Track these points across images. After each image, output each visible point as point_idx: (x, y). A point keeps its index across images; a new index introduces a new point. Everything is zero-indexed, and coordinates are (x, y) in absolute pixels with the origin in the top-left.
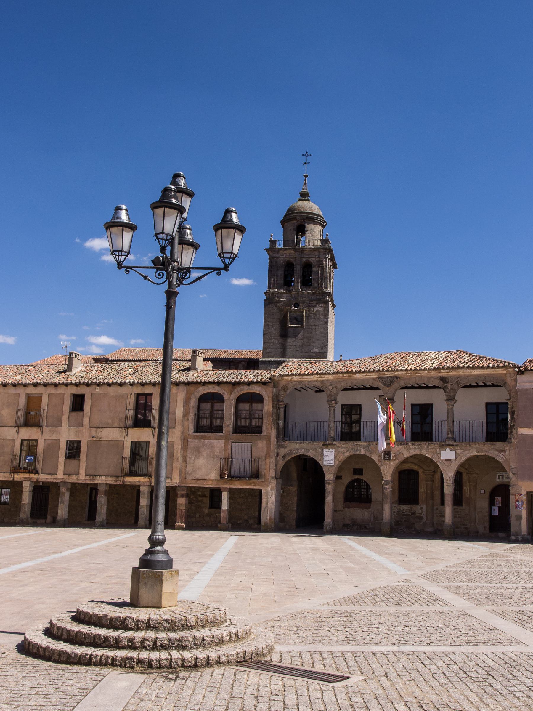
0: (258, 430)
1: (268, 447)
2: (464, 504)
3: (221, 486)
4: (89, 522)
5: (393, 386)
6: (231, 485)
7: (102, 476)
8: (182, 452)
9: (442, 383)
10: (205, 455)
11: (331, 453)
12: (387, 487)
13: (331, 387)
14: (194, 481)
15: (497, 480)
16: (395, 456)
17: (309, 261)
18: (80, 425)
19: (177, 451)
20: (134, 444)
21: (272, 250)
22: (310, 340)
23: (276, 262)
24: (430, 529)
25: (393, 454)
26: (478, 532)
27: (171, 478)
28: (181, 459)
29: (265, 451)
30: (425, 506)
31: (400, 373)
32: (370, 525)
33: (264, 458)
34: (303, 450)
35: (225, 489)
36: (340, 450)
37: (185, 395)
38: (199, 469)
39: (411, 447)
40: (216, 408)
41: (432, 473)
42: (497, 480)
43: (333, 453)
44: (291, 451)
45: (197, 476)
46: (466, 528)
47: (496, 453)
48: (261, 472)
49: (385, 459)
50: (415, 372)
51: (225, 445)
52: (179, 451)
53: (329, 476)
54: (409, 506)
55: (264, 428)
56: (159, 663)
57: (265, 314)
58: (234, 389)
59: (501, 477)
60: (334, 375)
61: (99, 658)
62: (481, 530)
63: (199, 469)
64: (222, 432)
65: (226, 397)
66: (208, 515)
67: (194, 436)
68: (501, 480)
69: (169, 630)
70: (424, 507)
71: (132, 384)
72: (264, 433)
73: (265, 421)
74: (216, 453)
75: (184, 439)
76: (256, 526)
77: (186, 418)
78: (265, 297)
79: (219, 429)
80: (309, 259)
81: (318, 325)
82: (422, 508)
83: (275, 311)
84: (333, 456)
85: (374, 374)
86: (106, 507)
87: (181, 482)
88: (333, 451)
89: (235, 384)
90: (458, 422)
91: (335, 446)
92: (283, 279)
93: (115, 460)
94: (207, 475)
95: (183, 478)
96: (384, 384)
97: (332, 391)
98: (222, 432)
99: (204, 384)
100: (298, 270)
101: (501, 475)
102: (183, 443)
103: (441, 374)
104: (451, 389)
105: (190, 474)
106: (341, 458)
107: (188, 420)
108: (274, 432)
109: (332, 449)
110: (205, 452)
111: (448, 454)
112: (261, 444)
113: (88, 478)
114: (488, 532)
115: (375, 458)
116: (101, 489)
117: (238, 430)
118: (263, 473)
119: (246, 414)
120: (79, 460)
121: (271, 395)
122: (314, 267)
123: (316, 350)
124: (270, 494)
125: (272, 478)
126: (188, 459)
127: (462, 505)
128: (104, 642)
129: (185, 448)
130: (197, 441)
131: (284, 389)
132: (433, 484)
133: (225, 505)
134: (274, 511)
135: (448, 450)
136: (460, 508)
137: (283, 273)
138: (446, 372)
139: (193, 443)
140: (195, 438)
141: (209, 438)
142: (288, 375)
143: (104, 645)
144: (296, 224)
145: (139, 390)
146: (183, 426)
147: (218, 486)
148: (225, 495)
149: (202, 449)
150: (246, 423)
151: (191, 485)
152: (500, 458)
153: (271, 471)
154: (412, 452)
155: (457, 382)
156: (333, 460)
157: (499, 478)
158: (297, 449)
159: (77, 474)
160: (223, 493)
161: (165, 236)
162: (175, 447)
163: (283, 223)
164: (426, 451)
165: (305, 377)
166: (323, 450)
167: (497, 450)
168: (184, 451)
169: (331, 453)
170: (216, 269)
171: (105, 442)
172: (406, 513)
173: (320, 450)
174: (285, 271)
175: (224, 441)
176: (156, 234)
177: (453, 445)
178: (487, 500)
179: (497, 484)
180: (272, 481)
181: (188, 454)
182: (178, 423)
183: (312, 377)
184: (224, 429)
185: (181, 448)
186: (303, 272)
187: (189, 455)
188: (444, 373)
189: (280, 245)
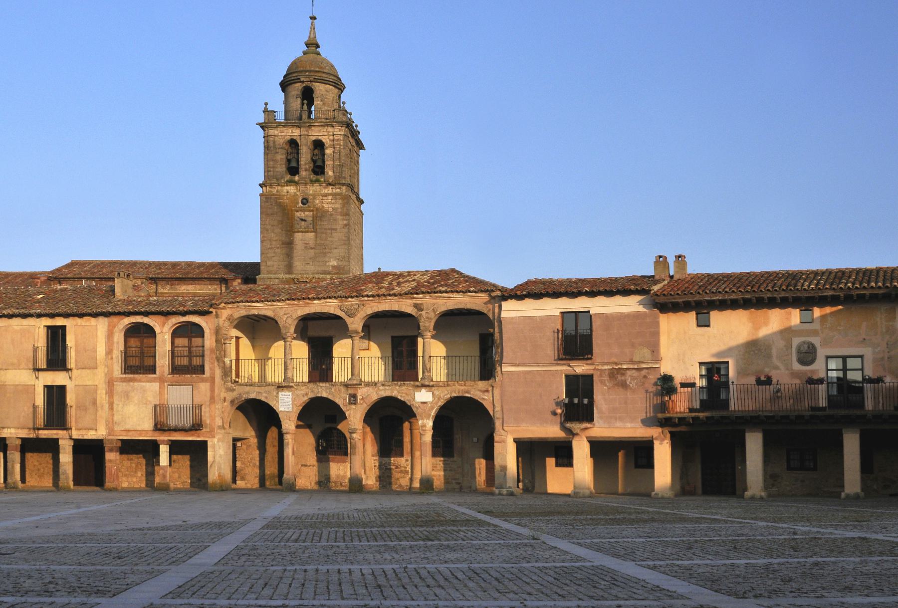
1: (212, 390)
7: (10, 428)
8: (107, 398)
10: (136, 402)
14: (124, 433)
16: (363, 399)
19: (101, 397)
20: (49, 389)
23: (274, 142)
25: (359, 397)
27: (96, 430)
28: (106, 406)
29: (208, 394)
33: (208, 403)
34: (255, 393)
38: (129, 417)
43: (291, 397)
44: (240, 394)
45: (128, 427)
47: (478, 393)
48: (205, 420)
49: (350, 403)
51: (160, 388)
52: (104, 396)
55: (207, 368)
57: (261, 213)
63: (129, 417)
64: (155, 373)
67: (122, 378)
73: (207, 359)
74: (149, 399)
75: (109, 382)
79: (152, 369)
80: (320, 138)
81: (335, 229)
83: (275, 210)
84: (290, 400)
87: (109, 434)
88: (290, 394)
90: (435, 358)
91: (293, 389)
92: (284, 166)
93: (26, 409)
94: (139, 425)
95: (111, 431)
97: (287, 321)
98: (155, 373)
102: (109, 387)
103: (415, 301)
104: (427, 318)
105: (119, 424)
108: (218, 373)
109: (289, 391)
110: (136, 397)
112: (204, 387)
115: (339, 401)
117: (176, 369)
118: (208, 422)
122: (327, 148)
126: (115, 406)
129: (110, 392)
130: (124, 384)
135: (423, 390)
137: (284, 157)
139: (119, 387)
140: (123, 380)
141: (140, 381)
146: (106, 366)
149: (132, 394)
150: (184, 361)
153: (217, 419)
156: (291, 406)
158: (248, 393)
162: (99, 392)
164: (399, 392)
166: (278, 393)
167: (481, 391)
168: (109, 397)
171: (12, 387)
173: (275, 394)
175: (158, 383)
177: (428, 386)
180: (218, 431)
182: (101, 362)
184: (157, 369)
185: (106, 393)
187: (116, 402)
189: (280, 117)
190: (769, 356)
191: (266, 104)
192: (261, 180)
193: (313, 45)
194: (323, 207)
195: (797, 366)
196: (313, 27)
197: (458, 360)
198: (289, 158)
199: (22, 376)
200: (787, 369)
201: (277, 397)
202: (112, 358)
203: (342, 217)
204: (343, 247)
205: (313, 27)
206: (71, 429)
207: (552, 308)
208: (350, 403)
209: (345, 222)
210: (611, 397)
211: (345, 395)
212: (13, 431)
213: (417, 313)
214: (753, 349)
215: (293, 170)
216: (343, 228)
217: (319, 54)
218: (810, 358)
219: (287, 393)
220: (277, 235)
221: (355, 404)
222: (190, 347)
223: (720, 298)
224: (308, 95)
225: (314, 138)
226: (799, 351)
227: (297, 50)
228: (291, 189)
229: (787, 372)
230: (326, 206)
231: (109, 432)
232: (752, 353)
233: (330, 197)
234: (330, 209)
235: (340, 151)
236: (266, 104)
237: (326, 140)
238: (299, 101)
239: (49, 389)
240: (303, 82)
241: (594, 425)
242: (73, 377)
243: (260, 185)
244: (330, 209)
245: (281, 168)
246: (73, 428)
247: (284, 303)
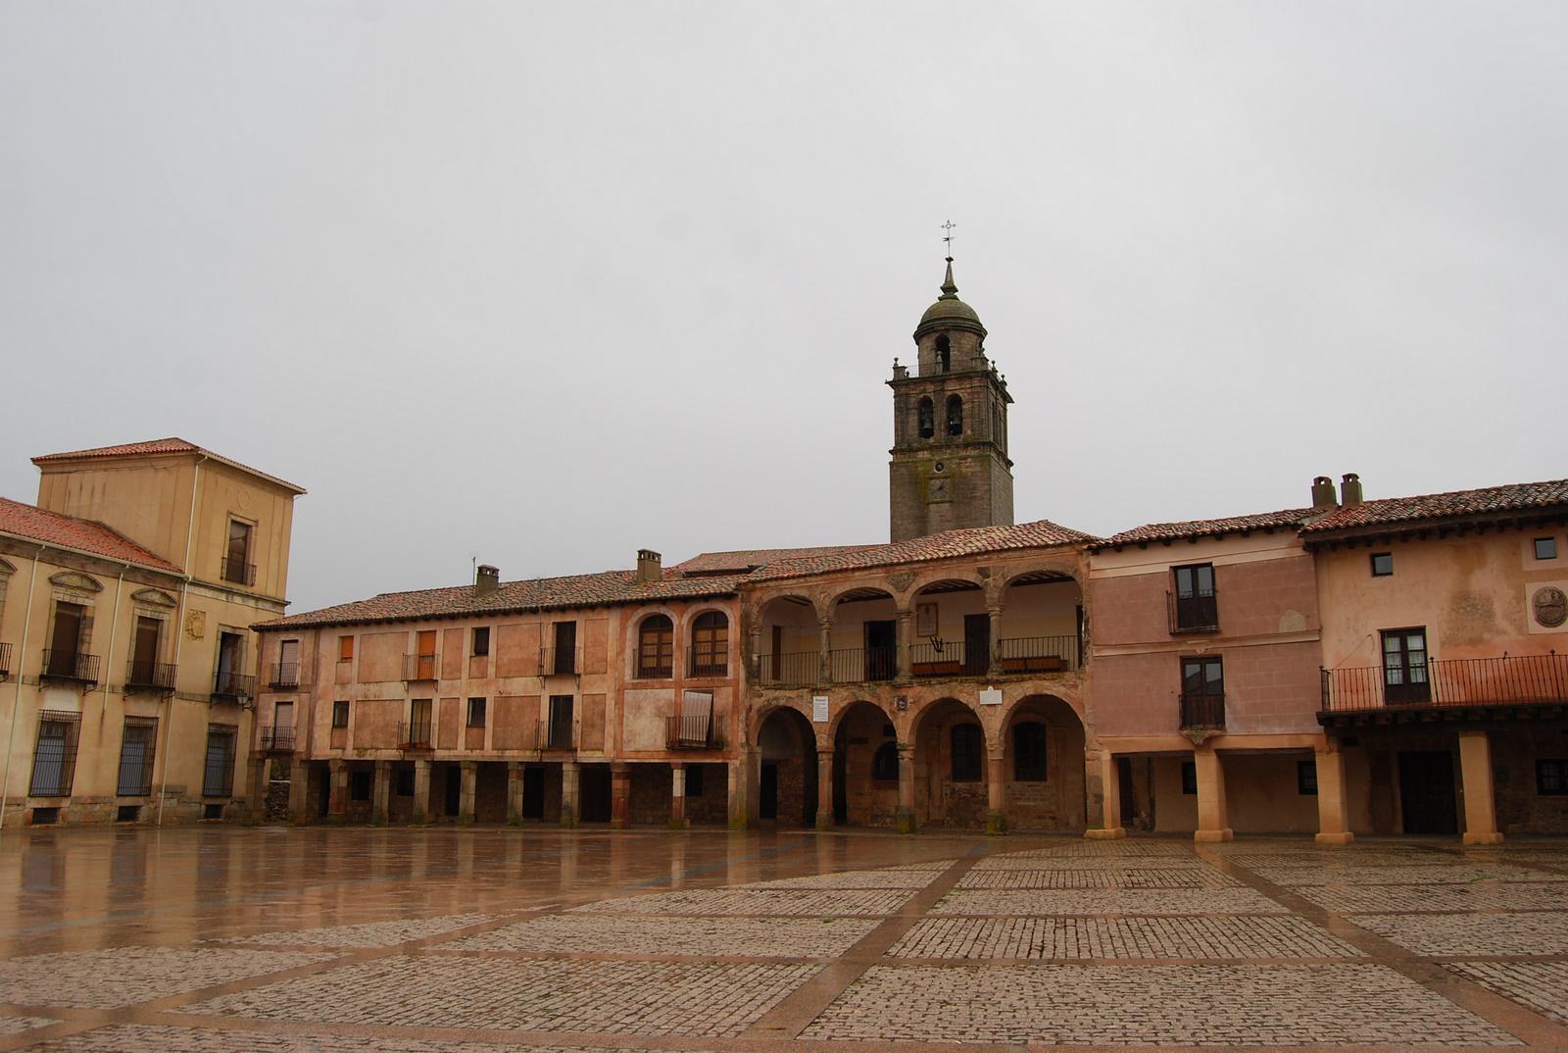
3: (671, 761)
6: (685, 758)
10: (648, 714)
13: (822, 596)
16: (914, 702)
17: (957, 395)
18: (483, 675)
20: (554, 699)
21: (900, 382)
25: (910, 700)
27: (603, 751)
33: (730, 713)
35: (677, 766)
43: (827, 702)
49: (900, 710)
53: (823, 741)
54: (968, 784)
60: (824, 577)
64: (671, 677)
67: (633, 684)
72: (730, 676)
77: (621, 657)
78: (891, 458)
80: (957, 392)
84: (827, 706)
85: (880, 570)
89: (685, 600)
90: (1006, 642)
92: (916, 428)
96: (896, 587)
98: (671, 677)
107: (624, 660)
108: (742, 674)
111: (990, 696)
113: (495, 753)
118: (730, 739)
119: (707, 648)
120: (484, 727)
121: (738, 615)
125: (742, 746)
127: (1045, 780)
129: (620, 703)
134: (745, 798)
135: (990, 688)
136: (1043, 783)
140: (635, 687)
142: (760, 581)
145: (559, 618)
147: (666, 761)
151: (629, 761)
153: (740, 734)
158: (776, 699)
159: (482, 748)
160: (675, 771)
163: (918, 337)
172: (963, 796)
190: (1489, 614)
191: (896, 360)
193: (949, 289)
194: (961, 471)
195: (1536, 628)
196: (949, 267)
197: (1046, 644)
199: (522, 685)
200: (1521, 634)
201: (812, 703)
205: (949, 267)
206: (576, 750)
207: (1159, 563)
210: (1249, 688)
212: (516, 751)
214: (1463, 604)
215: (927, 433)
217: (956, 298)
218: (1558, 615)
219: (823, 698)
223: (1404, 529)
224: (943, 346)
225: (949, 393)
226: (1538, 606)
227: (933, 296)
229: (1521, 637)
230: (964, 470)
232: (1461, 611)
234: (969, 474)
236: (896, 360)
239: (554, 699)
241: (1225, 731)
242: (581, 684)
243: (890, 452)
244: (969, 474)
246: (579, 749)
247: (820, 578)
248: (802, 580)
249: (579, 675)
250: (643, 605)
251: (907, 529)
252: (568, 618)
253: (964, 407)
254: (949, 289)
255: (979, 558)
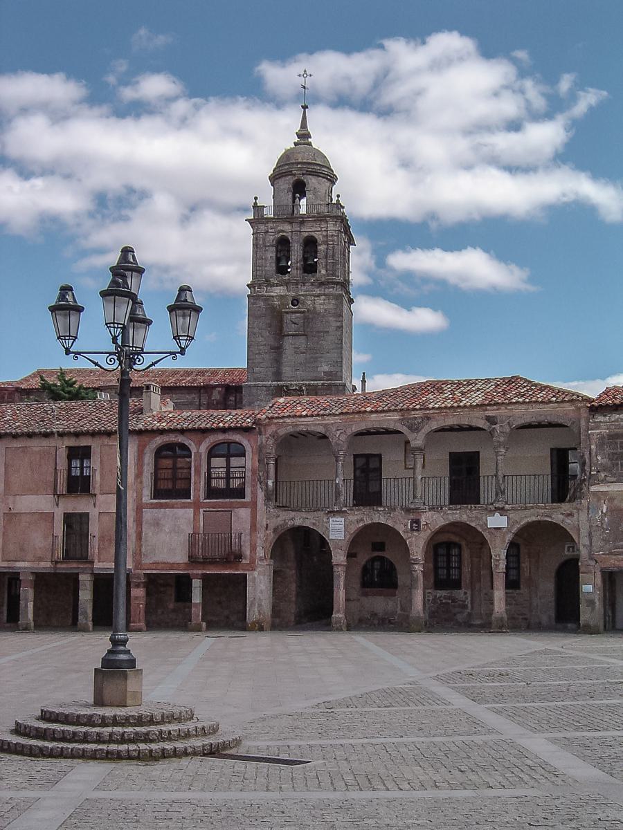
0: (240, 493)
2: (522, 586)
3: (190, 572)
4: (8, 625)
5: (423, 431)
9: (488, 424)
11: (341, 523)
12: (416, 567)
15: (566, 553)
17: (313, 237)
22: (317, 353)
24: (478, 622)
25: (423, 523)
26: (540, 623)
30: (470, 590)
31: (432, 411)
32: (396, 618)
35: (196, 576)
36: (351, 518)
37: (136, 448)
39: (449, 512)
40: (179, 465)
41: (480, 546)
42: (566, 553)
46: (526, 619)
49: (412, 530)
50: (452, 411)
51: (195, 514)
53: (339, 557)
54: (449, 591)
55: (248, 491)
56: (129, 754)
58: (205, 438)
59: (571, 548)
60: (342, 417)
61: (70, 750)
62: (545, 619)
64: (190, 498)
65: (193, 449)
66: (174, 611)
67: (152, 504)
68: (571, 553)
69: (135, 726)
70: (469, 592)
71: (61, 435)
72: (248, 499)
75: (137, 509)
76: (240, 624)
80: (313, 234)
81: (328, 332)
82: (465, 593)
84: (343, 526)
85: (395, 413)
86: (32, 603)
89: (205, 432)
92: (274, 265)
95: (138, 565)
96: (410, 428)
98: (190, 498)
99: (162, 432)
100: (297, 251)
101: (571, 547)
103: (487, 413)
106: (353, 528)
108: (261, 495)
111: (497, 521)
114: (554, 623)
115: (401, 529)
116: (26, 578)
117: (212, 493)
119: (221, 472)
122: (320, 245)
123: (326, 368)
124: (257, 580)
127: (519, 588)
128: (73, 737)
131: (274, 437)
132: (480, 561)
133: (197, 598)
137: (274, 255)
138: (494, 410)
142: (278, 418)
143: (73, 740)
144: (291, 182)
145: (72, 442)
148: (197, 584)
152: (568, 524)
154: (452, 518)
155: (508, 422)
157: (568, 550)
161: (116, 325)
165: (303, 419)
166: (328, 518)
168: (137, 525)
169: (341, 523)
170: (171, 353)
172: (444, 601)
174: (277, 251)
176: (106, 324)
178: (553, 580)
179: (565, 558)
181: (144, 530)
183: (312, 419)
186: (305, 252)
188: (491, 412)
189: (269, 213)
191: (256, 198)
192: (250, 280)
194: (315, 308)
198: (279, 256)
199: (43, 503)
202: (141, 482)
203: (335, 319)
204: (336, 351)
206: (93, 562)
208: (412, 530)
209: (339, 324)
211: (406, 521)
213: (489, 427)
215: (282, 270)
216: (336, 330)
217: (310, 144)
220: (266, 338)
221: (418, 530)
222: (228, 467)
225: (307, 234)
228: (279, 291)
231: (136, 566)
233: (323, 297)
235: (333, 248)
236: (256, 198)
237: (319, 236)
238: (290, 195)
239: (68, 518)
240: (294, 175)
242: (97, 503)
245: (271, 267)
246: (96, 561)
248: (320, 418)
249: (95, 495)
250: (161, 434)
251: (263, 359)
252: (83, 442)
253: (319, 248)
254: (304, 136)
255: (488, 407)
